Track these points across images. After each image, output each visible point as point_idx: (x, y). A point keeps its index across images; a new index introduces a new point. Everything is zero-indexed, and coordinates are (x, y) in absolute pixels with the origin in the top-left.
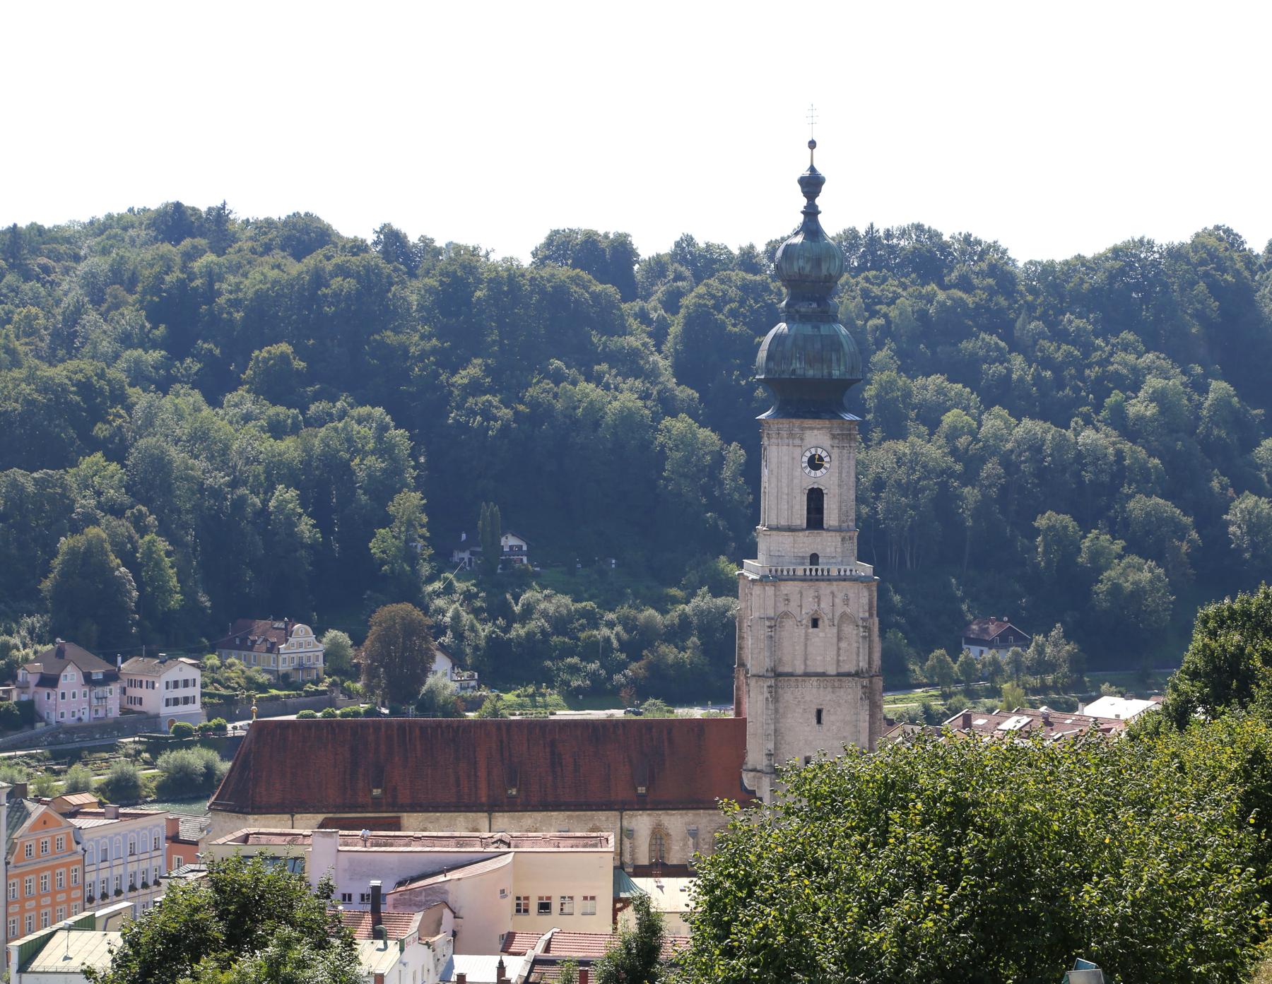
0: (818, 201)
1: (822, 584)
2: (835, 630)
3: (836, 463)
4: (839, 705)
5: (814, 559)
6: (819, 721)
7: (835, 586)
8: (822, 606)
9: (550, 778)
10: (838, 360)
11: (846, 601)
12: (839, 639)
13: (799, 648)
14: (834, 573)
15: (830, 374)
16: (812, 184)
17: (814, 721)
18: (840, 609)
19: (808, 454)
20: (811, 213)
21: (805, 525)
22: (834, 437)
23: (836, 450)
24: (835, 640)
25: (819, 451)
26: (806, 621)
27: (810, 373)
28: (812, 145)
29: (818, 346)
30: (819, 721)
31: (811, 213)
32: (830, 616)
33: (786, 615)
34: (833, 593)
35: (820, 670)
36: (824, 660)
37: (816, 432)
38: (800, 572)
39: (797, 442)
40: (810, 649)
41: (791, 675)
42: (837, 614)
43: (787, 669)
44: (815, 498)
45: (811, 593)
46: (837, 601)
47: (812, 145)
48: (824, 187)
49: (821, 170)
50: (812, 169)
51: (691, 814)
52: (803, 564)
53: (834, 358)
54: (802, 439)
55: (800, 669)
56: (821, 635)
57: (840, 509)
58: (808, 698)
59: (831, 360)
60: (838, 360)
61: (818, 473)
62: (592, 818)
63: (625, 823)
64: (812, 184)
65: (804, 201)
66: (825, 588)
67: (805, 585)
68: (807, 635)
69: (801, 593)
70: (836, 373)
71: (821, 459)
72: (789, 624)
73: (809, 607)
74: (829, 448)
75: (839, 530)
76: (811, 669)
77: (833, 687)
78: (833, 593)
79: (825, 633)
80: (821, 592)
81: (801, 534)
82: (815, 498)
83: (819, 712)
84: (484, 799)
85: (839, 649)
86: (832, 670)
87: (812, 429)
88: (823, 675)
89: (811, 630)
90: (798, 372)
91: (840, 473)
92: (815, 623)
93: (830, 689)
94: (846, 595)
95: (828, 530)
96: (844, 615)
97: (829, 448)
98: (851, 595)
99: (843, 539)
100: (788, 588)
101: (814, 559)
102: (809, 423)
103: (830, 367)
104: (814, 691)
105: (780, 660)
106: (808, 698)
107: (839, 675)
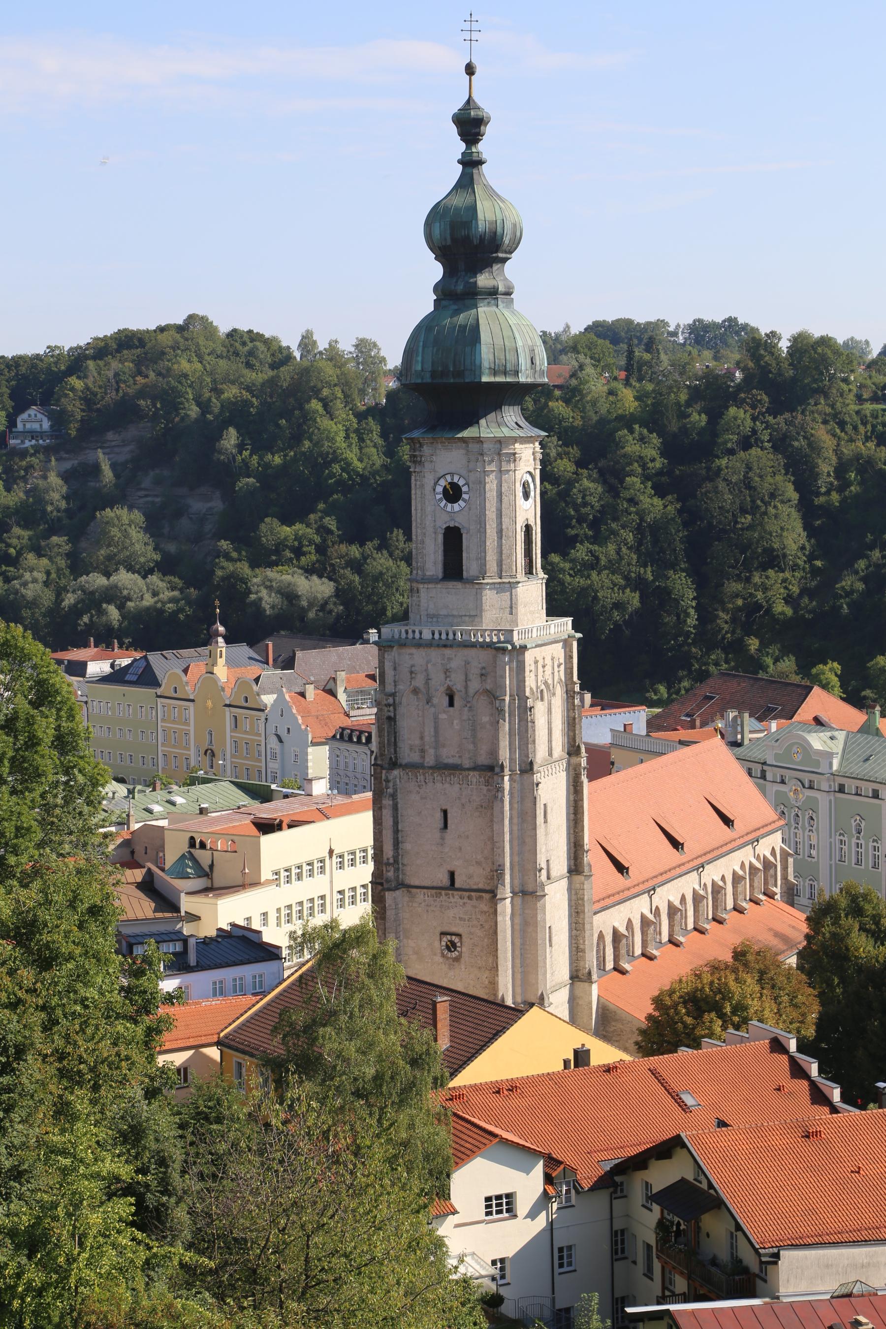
16: (470, 125)
28: (470, 70)
47: (470, 70)
50: (469, 101)
64: (470, 125)
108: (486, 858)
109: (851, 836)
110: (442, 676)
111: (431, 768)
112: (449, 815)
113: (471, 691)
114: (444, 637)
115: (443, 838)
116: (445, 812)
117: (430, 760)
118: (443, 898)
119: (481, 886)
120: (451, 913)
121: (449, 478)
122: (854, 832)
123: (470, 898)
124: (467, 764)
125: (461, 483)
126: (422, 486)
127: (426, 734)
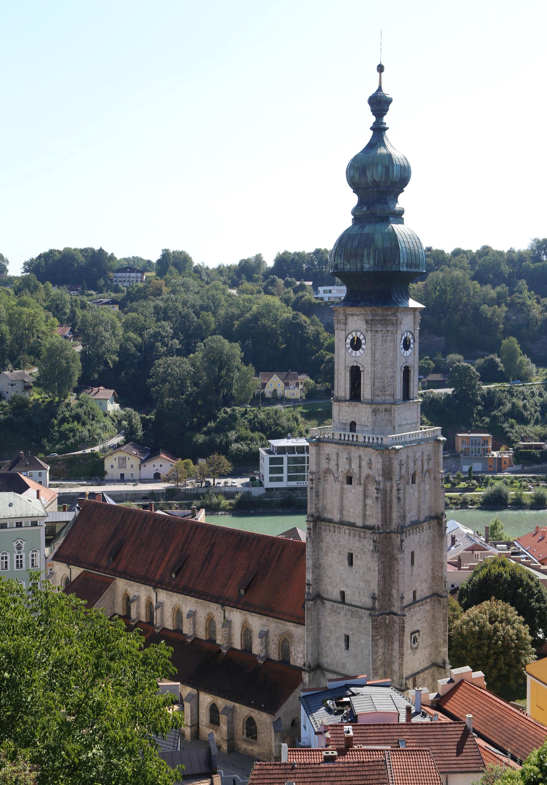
0: (386, 119)
1: (353, 448)
2: (361, 488)
3: (369, 345)
4: (364, 553)
5: (353, 426)
6: (351, 563)
7: (362, 451)
9: (198, 570)
10: (369, 255)
11: (370, 463)
12: (365, 496)
13: (336, 500)
14: (361, 439)
15: (362, 267)
16: (379, 104)
17: (346, 562)
18: (365, 471)
19: (350, 337)
20: (379, 130)
21: (348, 397)
22: (367, 322)
23: (369, 333)
24: (361, 497)
25: (359, 333)
27: (348, 267)
28: (381, 69)
29: (356, 243)
30: (351, 563)
31: (379, 130)
32: (358, 476)
33: (328, 471)
34: (360, 457)
35: (352, 520)
36: (354, 514)
37: (355, 318)
38: (337, 437)
39: (343, 327)
40: (345, 502)
41: (331, 521)
42: (364, 475)
44: (355, 373)
45: (344, 456)
46: (364, 464)
47: (381, 69)
48: (391, 107)
49: (386, 90)
50: (380, 89)
51: (265, 618)
52: (344, 430)
53: (365, 254)
54: (345, 324)
55: (336, 517)
56: (353, 491)
57: (373, 385)
59: (363, 255)
60: (369, 255)
61: (358, 352)
62: (209, 607)
63: (227, 615)
64: (379, 104)
65: (374, 119)
66: (355, 452)
67: (341, 447)
68: (342, 490)
69: (338, 455)
70: (366, 266)
71: (353, 340)
72: (330, 478)
73: (344, 467)
74: (364, 332)
75: (371, 403)
78: (360, 457)
79: (354, 492)
80: (352, 455)
81: (344, 404)
82: (355, 373)
83: (350, 557)
84: (157, 578)
85: (365, 505)
86: (359, 523)
87: (353, 315)
89: (346, 486)
90: (340, 266)
91: (373, 354)
92: (349, 480)
93: (357, 538)
95: (363, 402)
96: (367, 477)
97: (364, 332)
98: (373, 460)
99: (375, 412)
100: (329, 449)
101: (353, 426)
102: (350, 310)
103: (362, 261)
104: (346, 537)
105: (325, 508)
106: (342, 542)
107: (365, 527)
108: (428, 576)
109: (12, 553)
110: (413, 464)
111: (409, 526)
112: (415, 555)
113: (424, 471)
114: (371, 441)
115: (412, 571)
116: (413, 554)
117: (408, 522)
118: (412, 610)
119: (426, 595)
120: (414, 619)
121: (354, 333)
122: (16, 550)
123: (422, 605)
124: (422, 519)
125: (361, 337)
126: (394, 340)
127: (407, 504)
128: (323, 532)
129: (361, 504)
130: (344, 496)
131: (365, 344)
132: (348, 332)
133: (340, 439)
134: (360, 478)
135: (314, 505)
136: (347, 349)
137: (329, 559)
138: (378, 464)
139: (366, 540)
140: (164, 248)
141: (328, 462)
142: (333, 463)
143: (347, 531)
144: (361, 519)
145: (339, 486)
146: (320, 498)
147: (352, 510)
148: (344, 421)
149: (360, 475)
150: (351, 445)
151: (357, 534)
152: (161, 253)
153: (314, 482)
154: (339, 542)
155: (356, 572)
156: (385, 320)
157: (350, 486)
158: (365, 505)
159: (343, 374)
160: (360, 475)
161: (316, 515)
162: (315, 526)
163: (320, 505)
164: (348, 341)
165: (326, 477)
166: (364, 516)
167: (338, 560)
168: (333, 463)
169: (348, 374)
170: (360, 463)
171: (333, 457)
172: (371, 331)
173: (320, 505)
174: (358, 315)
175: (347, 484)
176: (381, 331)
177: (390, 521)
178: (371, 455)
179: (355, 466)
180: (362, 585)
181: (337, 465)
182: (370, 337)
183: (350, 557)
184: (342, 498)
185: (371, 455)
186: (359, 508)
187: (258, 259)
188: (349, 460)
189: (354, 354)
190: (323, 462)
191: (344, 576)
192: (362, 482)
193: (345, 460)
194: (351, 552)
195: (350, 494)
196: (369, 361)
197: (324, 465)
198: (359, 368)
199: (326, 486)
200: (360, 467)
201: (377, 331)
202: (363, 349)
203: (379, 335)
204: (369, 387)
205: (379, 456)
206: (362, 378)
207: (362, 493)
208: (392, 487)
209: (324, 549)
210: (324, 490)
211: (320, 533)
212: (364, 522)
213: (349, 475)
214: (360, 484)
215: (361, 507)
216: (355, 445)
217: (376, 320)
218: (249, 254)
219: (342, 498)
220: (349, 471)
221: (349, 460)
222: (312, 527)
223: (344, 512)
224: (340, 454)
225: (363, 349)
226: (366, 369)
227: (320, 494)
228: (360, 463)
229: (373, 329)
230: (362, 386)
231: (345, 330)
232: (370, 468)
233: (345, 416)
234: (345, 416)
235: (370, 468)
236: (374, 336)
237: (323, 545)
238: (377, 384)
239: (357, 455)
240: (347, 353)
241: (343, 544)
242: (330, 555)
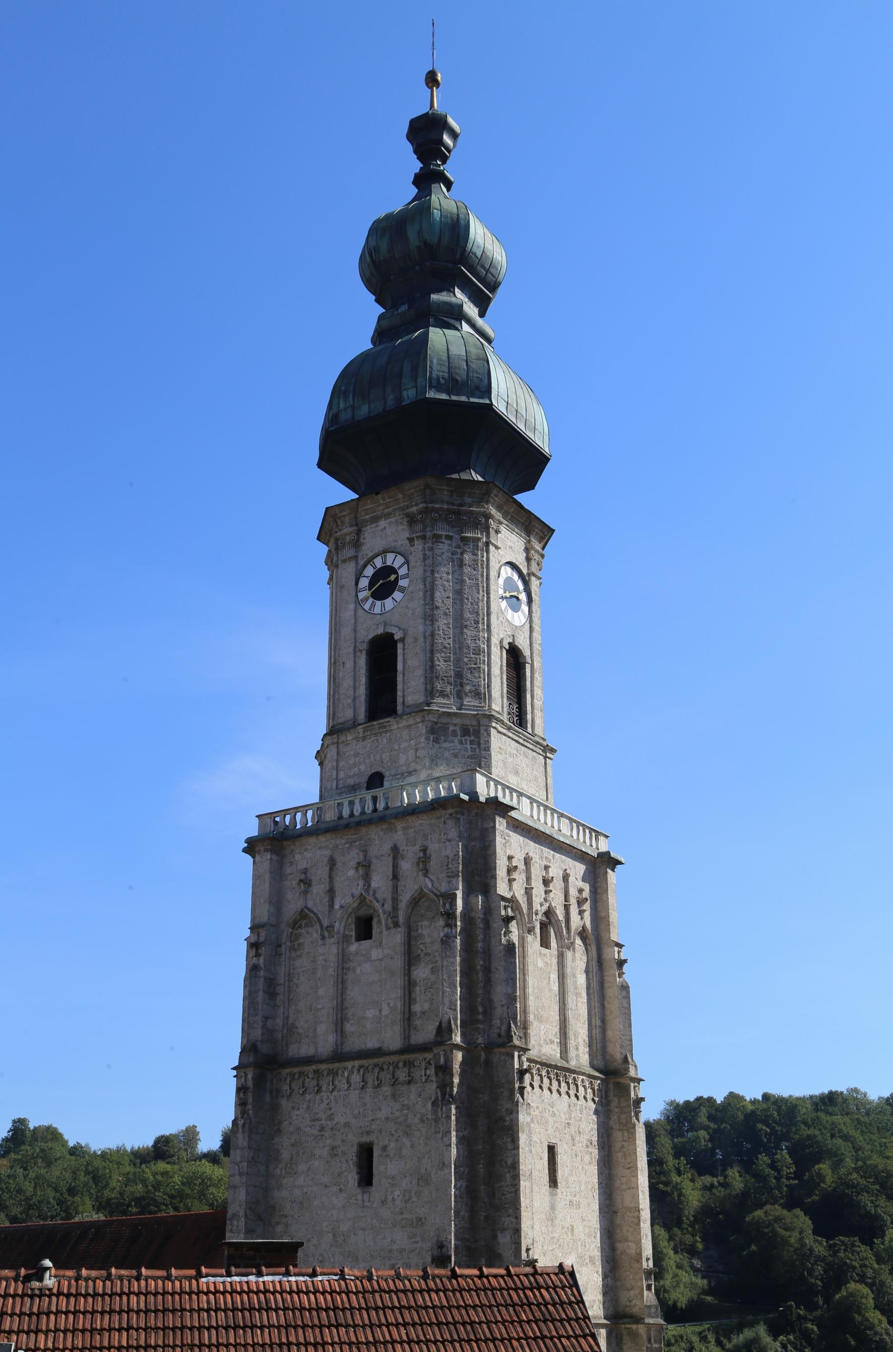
2: (397, 937)
6: (366, 1179)
8: (374, 885)
13: (326, 992)
15: (399, 399)
17: (352, 1177)
19: (369, 571)
22: (412, 521)
23: (418, 545)
24: (398, 963)
26: (343, 925)
27: (364, 411)
30: (366, 1179)
32: (388, 907)
33: (304, 917)
37: (382, 523)
40: (354, 994)
41: (309, 1061)
42: (405, 898)
43: (304, 1050)
46: (406, 866)
56: (375, 954)
58: (340, 1119)
61: (389, 603)
67: (340, 841)
68: (344, 961)
69: (332, 863)
72: (310, 936)
76: (353, 1044)
77: (395, 1082)
78: (395, 850)
80: (374, 851)
83: (365, 1158)
85: (410, 985)
88: (378, 1053)
89: (354, 947)
90: (343, 417)
93: (386, 1089)
94: (424, 850)
96: (415, 902)
104: (354, 1095)
105: (291, 1028)
106: (340, 1119)
128: (284, 1102)
129: (399, 981)
130: (350, 977)
131: (406, 576)
132: (361, 562)
133: (341, 817)
134: (395, 908)
135: (259, 1018)
136: (359, 603)
137: (300, 1181)
138: (449, 845)
139: (413, 1088)
140: (16, 1117)
141: (306, 893)
142: (319, 889)
143: (356, 1078)
144: (398, 1028)
145: (334, 950)
146: (279, 998)
147: (370, 1014)
148: (351, 782)
149: (395, 900)
150: (370, 822)
151: (386, 1076)
152: (9, 1125)
153: (263, 950)
154: (330, 1118)
155: (384, 1202)
156: (458, 513)
157: (366, 943)
158: (410, 985)
159: (349, 664)
160: (395, 900)
161: (265, 1049)
162: (259, 1080)
163: (279, 1021)
164: (364, 582)
165: (298, 936)
166: (408, 1018)
167: (325, 1179)
168: (319, 889)
169: (362, 661)
170: (395, 867)
171: (320, 874)
172: (424, 537)
173: (279, 1021)
174: (387, 516)
175: (359, 939)
176: (449, 538)
177: (485, 1013)
178: (425, 836)
179: (380, 881)
180: (401, 1239)
181: (331, 892)
182: (420, 555)
183: (365, 1158)
184: (341, 985)
185: (425, 836)
186: (392, 998)
187: (191, 1135)
188: (365, 867)
189: (377, 610)
190: (289, 895)
191: (344, 1227)
192: (401, 919)
193: (351, 873)
194: (366, 1139)
195: (367, 967)
196: (419, 611)
197: (293, 904)
198: (392, 635)
199: (298, 963)
200: (395, 877)
201: (437, 538)
202: (402, 589)
203: (444, 548)
204: (420, 672)
205: (450, 823)
206: (400, 658)
207: (400, 949)
208: (489, 910)
209: (285, 1155)
210: (290, 976)
211: (275, 1108)
212: (407, 1037)
213: (363, 912)
214: (396, 925)
215: (399, 993)
216: (382, 819)
217: (436, 510)
218: (172, 1127)
219: (341, 985)
220: (362, 900)
221: (365, 867)
222: (250, 1083)
223: (349, 1027)
224: (339, 859)
225: (402, 589)
226: (411, 632)
227: (280, 990)
228: (395, 867)
229: (429, 534)
230: (400, 678)
231: (356, 558)
232: (426, 872)
233: (354, 765)
234: (354, 765)
235: (426, 872)
236: (431, 549)
237: (284, 1143)
238: (441, 665)
239: (387, 848)
240: (360, 612)
241: (342, 1121)
242: (302, 1167)
